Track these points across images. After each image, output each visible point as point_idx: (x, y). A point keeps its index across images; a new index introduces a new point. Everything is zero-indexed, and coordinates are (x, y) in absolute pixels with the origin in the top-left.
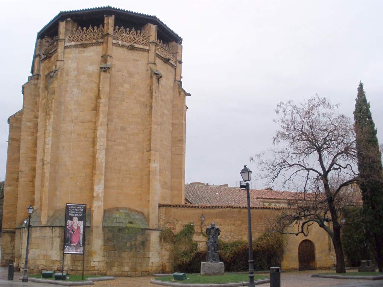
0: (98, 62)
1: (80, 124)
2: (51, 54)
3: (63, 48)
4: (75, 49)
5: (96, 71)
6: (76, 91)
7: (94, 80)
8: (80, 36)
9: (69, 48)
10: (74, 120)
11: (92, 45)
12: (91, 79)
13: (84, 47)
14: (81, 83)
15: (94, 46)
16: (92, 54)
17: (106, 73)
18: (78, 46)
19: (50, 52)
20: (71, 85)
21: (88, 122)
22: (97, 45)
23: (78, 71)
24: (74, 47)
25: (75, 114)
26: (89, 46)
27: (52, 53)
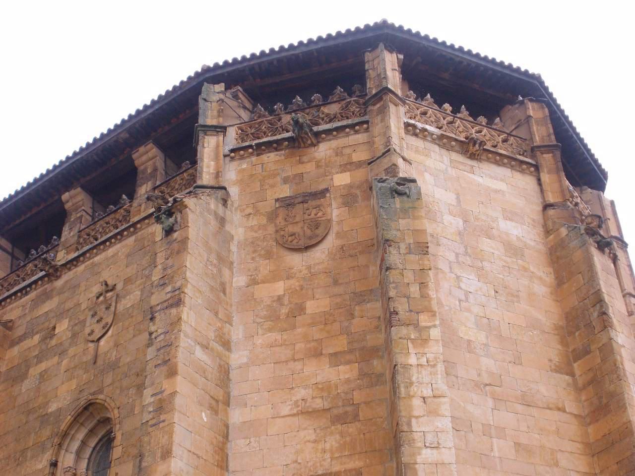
0: (533, 220)
1: (520, 408)
2: (317, 134)
3: (403, 126)
4: (437, 148)
5: (532, 244)
6: (471, 282)
7: (532, 268)
8: (444, 119)
9: (416, 135)
10: (490, 385)
11: (499, 160)
12: (520, 262)
13: (473, 157)
14: (485, 264)
15: (504, 165)
16: (502, 186)
17: (602, 254)
18: (453, 143)
19: (315, 129)
20: (452, 257)
21: (550, 409)
22: (512, 167)
23: (465, 221)
24: (433, 141)
25: (487, 363)
26: (488, 160)
27: (328, 132)
